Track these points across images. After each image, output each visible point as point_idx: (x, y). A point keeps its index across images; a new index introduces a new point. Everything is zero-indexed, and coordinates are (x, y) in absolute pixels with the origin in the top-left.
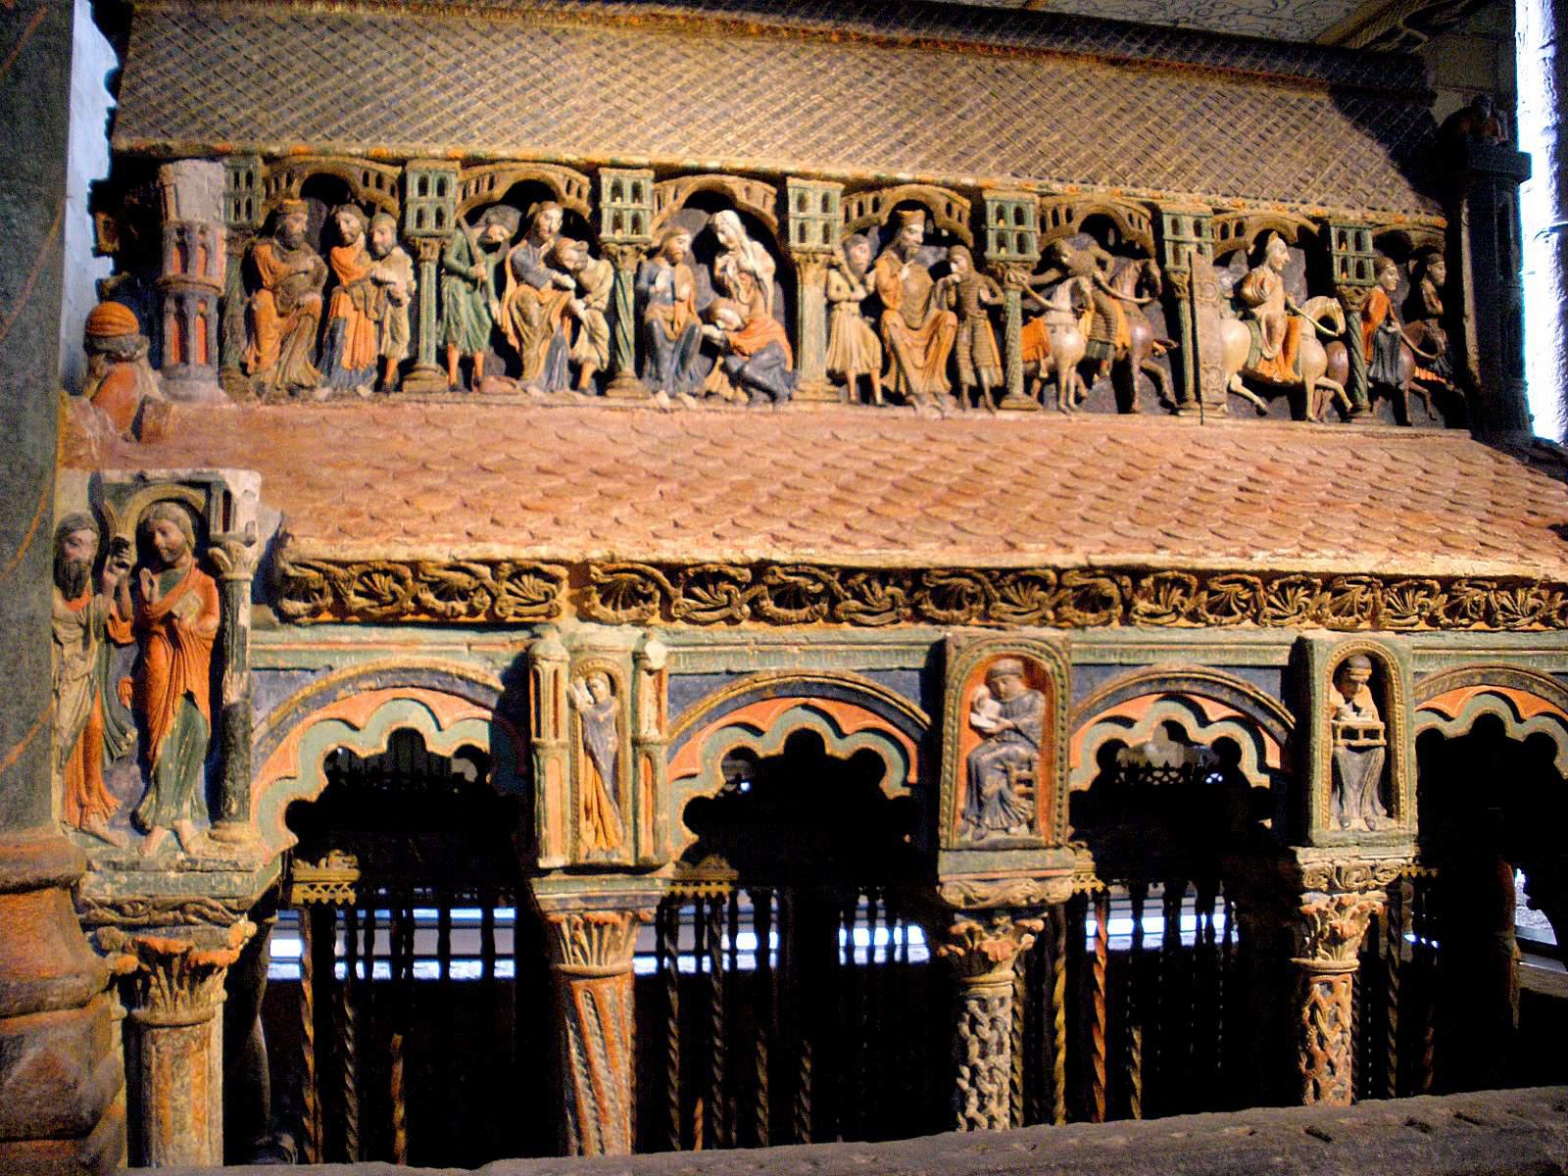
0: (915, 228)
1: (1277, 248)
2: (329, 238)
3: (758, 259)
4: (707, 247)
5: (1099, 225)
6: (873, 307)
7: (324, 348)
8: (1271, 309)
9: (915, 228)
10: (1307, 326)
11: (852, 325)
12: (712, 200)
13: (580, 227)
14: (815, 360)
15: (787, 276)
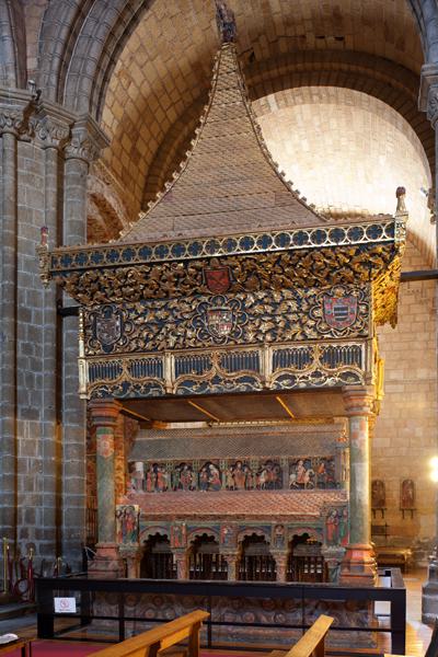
0: (239, 465)
1: (301, 463)
2: (155, 471)
3: (216, 471)
4: (208, 471)
5: (269, 461)
6: (233, 476)
7: (156, 485)
8: (300, 473)
9: (239, 465)
10: (307, 474)
11: (230, 479)
12: (209, 463)
13: (190, 468)
14: (224, 485)
15: (220, 473)
